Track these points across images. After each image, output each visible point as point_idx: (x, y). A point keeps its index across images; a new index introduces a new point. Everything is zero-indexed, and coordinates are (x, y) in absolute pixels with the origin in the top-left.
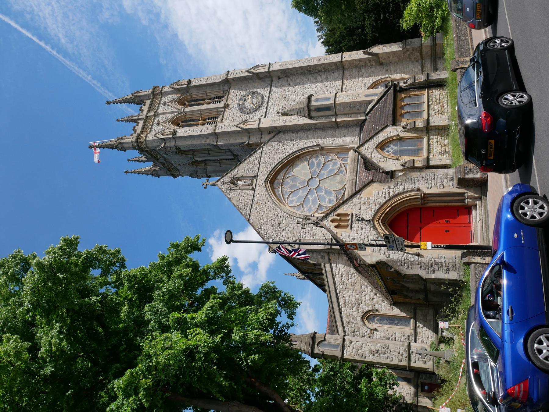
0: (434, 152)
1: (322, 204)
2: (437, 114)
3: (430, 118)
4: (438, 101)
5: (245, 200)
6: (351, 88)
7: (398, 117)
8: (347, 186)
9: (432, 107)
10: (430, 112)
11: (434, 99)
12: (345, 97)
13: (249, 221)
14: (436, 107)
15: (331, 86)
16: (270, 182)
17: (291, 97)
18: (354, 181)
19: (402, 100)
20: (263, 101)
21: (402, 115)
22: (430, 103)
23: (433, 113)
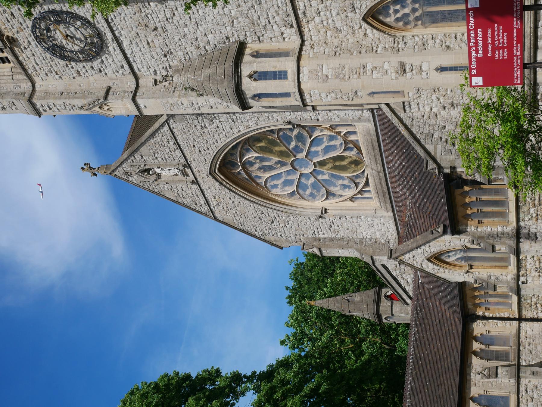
0: (528, 266)
1: (332, 189)
2: (534, 219)
3: (522, 224)
4: (537, 202)
5: (190, 195)
6: (319, 13)
7: (460, 219)
8: (369, 172)
9: (524, 209)
10: (521, 216)
11: (528, 200)
12: (323, 95)
13: (215, 219)
14: (532, 211)
15: (265, 6)
16: (219, 171)
17: (169, 27)
18: (382, 174)
19: (466, 194)
20: (100, 35)
21: (468, 217)
22: (521, 204)
23: (526, 218)
